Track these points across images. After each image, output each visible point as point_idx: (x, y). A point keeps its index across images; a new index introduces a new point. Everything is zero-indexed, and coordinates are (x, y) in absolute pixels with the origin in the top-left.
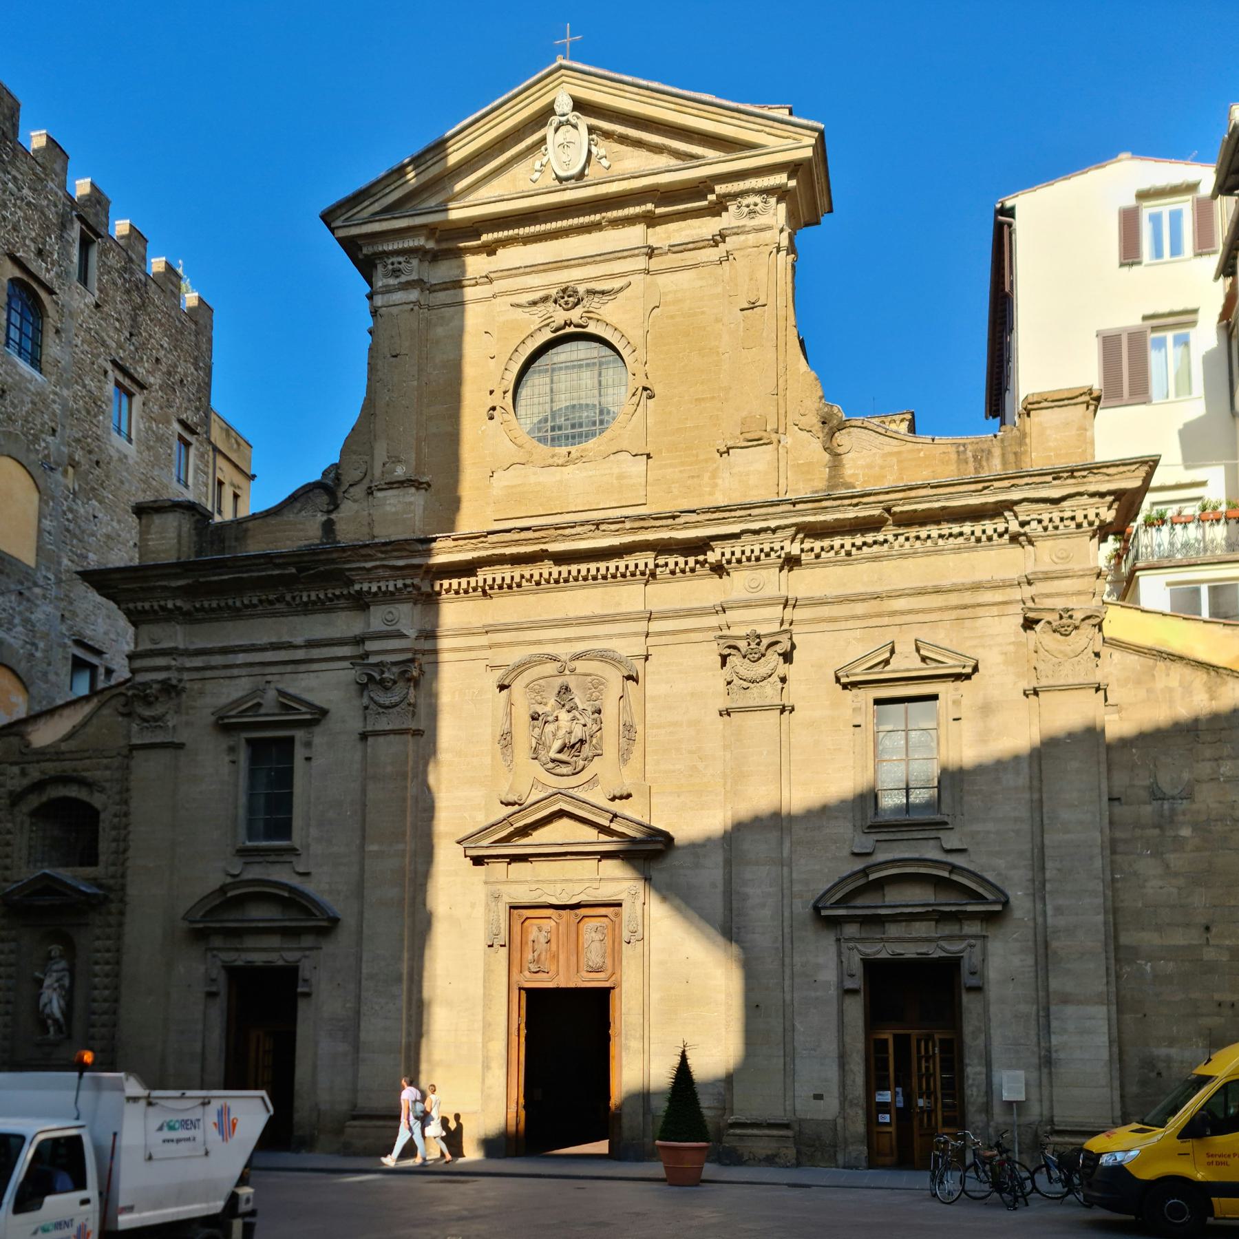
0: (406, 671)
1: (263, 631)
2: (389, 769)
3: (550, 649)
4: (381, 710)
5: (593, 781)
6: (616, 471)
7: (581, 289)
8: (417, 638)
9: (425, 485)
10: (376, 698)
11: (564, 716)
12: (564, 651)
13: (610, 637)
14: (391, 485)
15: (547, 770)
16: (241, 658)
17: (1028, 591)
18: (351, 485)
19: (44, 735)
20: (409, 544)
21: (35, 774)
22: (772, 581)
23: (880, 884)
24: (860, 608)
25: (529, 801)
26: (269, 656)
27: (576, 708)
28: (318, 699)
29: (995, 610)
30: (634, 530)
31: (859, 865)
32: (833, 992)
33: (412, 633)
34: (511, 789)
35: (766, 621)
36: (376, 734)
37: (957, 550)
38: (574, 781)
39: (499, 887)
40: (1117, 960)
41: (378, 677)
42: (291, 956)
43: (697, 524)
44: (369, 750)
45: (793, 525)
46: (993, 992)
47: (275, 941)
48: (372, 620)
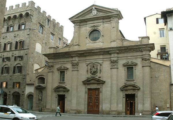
1: (62, 60)
3: (92, 62)
5: (97, 76)
7: (96, 26)
11: (93, 69)
12: (94, 62)
14: (76, 45)
16: (59, 63)
17: (142, 56)
19: (39, 71)
21: (39, 75)
22: (116, 55)
23: (127, 86)
24: (125, 58)
26: (62, 63)
28: (68, 67)
29: (139, 58)
30: (101, 50)
31: (125, 84)
32: (122, 97)
33: (78, 60)
35: (115, 59)
37: (135, 52)
38: (95, 76)
40: (151, 94)
42: (64, 94)
43: (107, 49)
46: (138, 97)
47: (63, 92)
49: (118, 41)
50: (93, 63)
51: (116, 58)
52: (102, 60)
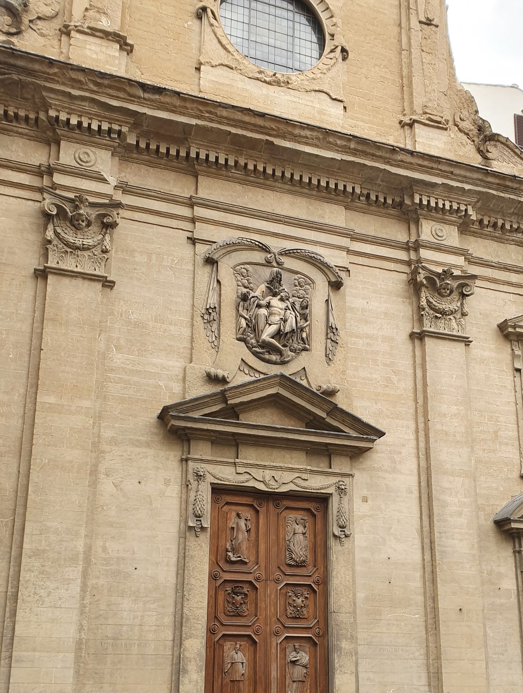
2: (74, 315)
4: (69, 250)
8: (116, 187)
9: (129, 48)
14: (93, 32)
15: (255, 354)
18: (39, 18)
30: (355, 152)
33: (113, 181)
39: (203, 465)
44: (49, 289)
45: (479, 193)
50: (265, 249)
52: (345, 242)
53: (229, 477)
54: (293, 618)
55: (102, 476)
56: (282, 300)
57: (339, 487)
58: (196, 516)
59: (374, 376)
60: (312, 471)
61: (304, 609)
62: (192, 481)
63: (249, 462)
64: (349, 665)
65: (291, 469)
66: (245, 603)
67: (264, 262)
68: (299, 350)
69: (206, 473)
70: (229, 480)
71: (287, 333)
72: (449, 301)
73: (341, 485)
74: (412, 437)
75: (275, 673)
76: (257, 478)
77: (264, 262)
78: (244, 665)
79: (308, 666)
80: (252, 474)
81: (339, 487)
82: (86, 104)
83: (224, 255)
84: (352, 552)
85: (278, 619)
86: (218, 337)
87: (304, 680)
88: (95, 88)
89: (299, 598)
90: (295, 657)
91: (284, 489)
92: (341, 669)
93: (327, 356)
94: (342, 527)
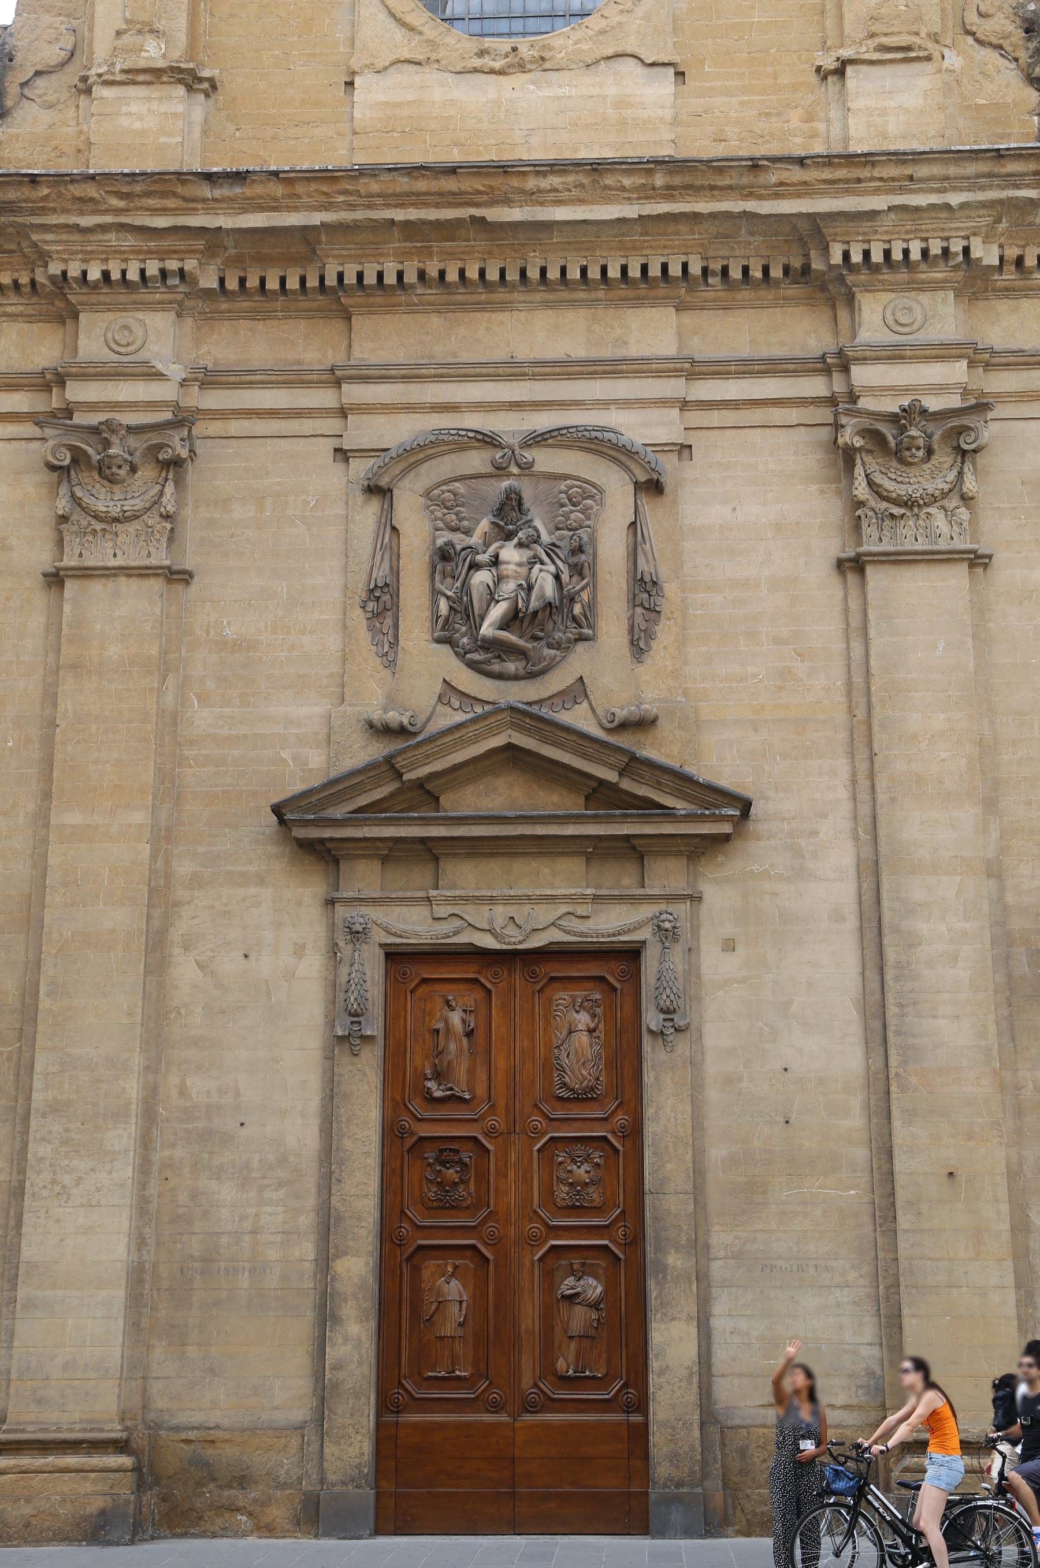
0: (160, 447)
4: (98, 526)
5: (579, 690)
6: (611, 90)
8: (184, 383)
10: (87, 500)
13: (605, 404)
15: (472, 665)
20: (183, 182)
25: (433, 728)
27: (537, 540)
33: (176, 371)
34: (391, 702)
36: (85, 573)
39: (365, 910)
41: (95, 457)
43: (804, 190)
44: (67, 608)
48: (82, 341)
49: (953, 60)
50: (488, 440)
51: (958, 371)
52: (673, 387)
53: (419, 929)
54: (568, 1207)
55: (177, 951)
56: (520, 545)
57: (659, 927)
58: (351, 1015)
59: (750, 669)
60: (596, 898)
61: (591, 1190)
62: (341, 944)
63: (458, 893)
64: (682, 1301)
65: (551, 899)
66: (462, 1181)
67: (490, 469)
68: (569, 641)
69: (369, 926)
70: (417, 935)
71: (535, 613)
72: (928, 472)
73: (663, 921)
74: (843, 794)
75: (530, 1322)
76: (477, 925)
77: (490, 469)
78: (464, 1305)
79: (602, 1306)
80: (466, 917)
81: (659, 927)
82: (112, 236)
83: (404, 472)
84: (696, 1064)
85: (535, 1212)
86: (394, 644)
87: (592, 1333)
88: (122, 204)
89: (579, 1167)
90: (572, 1288)
91: (537, 942)
92: (664, 1311)
93: (633, 643)
94: (668, 1011)
